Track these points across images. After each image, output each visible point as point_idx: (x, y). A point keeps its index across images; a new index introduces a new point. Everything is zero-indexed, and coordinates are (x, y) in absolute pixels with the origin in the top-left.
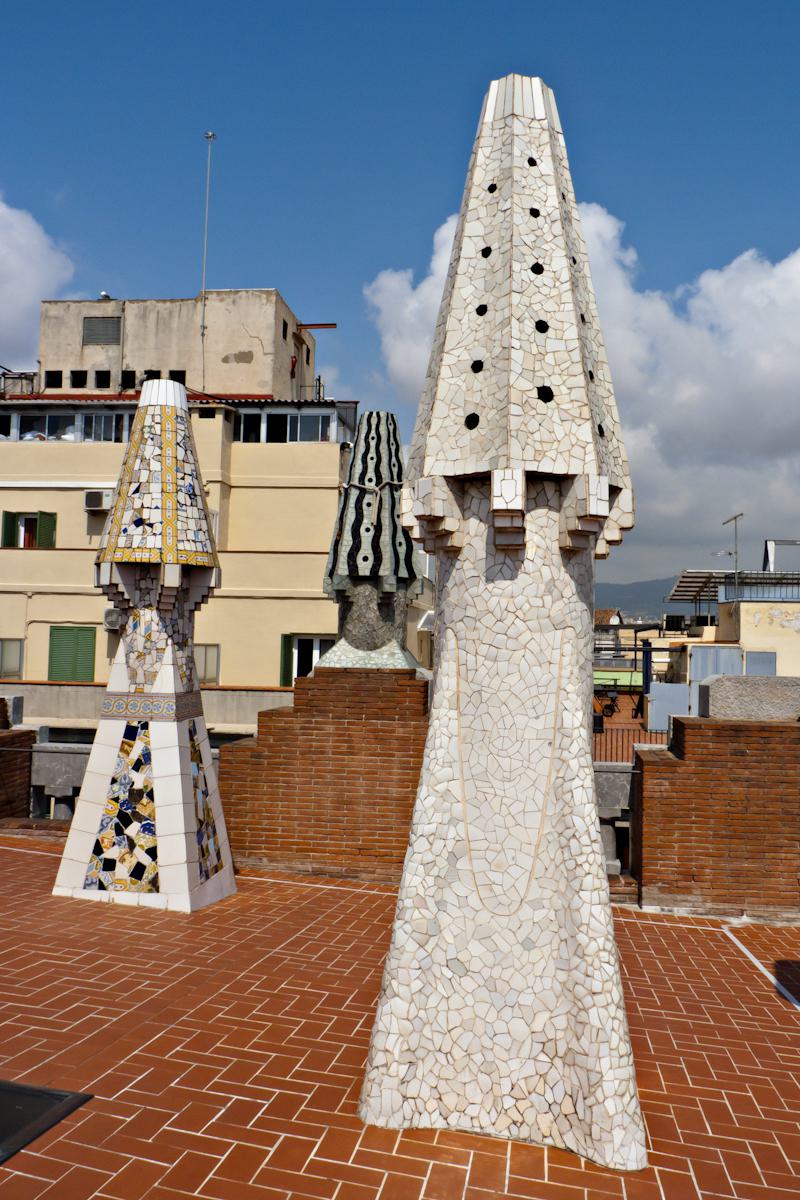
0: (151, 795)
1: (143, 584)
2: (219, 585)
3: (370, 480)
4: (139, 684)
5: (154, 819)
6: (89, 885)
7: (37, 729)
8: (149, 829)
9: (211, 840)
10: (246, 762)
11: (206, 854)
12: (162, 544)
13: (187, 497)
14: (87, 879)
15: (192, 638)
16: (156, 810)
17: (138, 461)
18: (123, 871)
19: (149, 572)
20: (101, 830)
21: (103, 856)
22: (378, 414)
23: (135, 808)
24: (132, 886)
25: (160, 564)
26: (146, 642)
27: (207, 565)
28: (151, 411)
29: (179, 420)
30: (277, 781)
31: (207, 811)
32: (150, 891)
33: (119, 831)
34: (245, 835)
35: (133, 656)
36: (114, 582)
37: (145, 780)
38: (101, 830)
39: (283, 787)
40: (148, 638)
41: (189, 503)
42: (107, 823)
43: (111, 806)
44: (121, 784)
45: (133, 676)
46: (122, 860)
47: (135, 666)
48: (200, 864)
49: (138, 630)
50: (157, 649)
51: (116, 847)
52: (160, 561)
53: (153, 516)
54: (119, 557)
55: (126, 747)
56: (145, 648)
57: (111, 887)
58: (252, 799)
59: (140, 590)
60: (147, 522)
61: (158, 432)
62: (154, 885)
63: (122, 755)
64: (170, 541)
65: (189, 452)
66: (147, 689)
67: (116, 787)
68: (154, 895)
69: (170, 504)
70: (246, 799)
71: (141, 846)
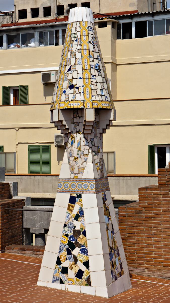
0: (84, 233)
1: (75, 120)
2: (115, 119)
4: (76, 174)
5: (87, 246)
6: (55, 281)
7: (25, 199)
8: (84, 251)
9: (117, 258)
10: (133, 216)
11: (115, 266)
12: (84, 98)
13: (96, 71)
14: (54, 278)
15: (102, 148)
16: (88, 241)
17: (69, 53)
18: (72, 274)
19: (78, 113)
20: (60, 251)
21: (61, 265)
23: (77, 240)
24: (77, 282)
25: (83, 109)
26: (78, 151)
27: (108, 108)
28: (74, 25)
29: (90, 29)
30: (151, 227)
31: (114, 242)
32: (86, 285)
33: (69, 253)
34: (134, 256)
35: (72, 159)
36: (60, 120)
37: (81, 225)
38: (60, 251)
39: (154, 230)
40: (79, 149)
41: (97, 75)
42: (63, 248)
43: (64, 239)
44: (69, 227)
45: (72, 169)
46: (71, 268)
47: (73, 165)
48: (112, 271)
49: (74, 145)
50: (84, 155)
51: (68, 261)
52: (83, 107)
53: (79, 83)
54: (62, 106)
55: (71, 207)
56: (78, 154)
57: (66, 282)
58: (138, 236)
59: (74, 123)
60: (76, 86)
61: (79, 37)
62: (88, 282)
63: (69, 212)
64: (88, 96)
65: (95, 46)
66: (80, 176)
67: (66, 229)
68: (88, 287)
69: (87, 76)
70: (134, 236)
71: (80, 260)
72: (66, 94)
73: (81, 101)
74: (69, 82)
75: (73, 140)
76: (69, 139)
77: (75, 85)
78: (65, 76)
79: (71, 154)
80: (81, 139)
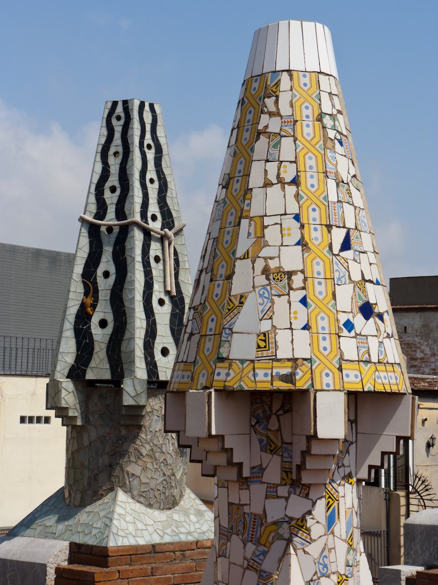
3: (154, 218)
17: (332, 184)
22: (152, 106)
26: (348, 552)
72: (357, 334)
73: (396, 365)
74: (357, 290)
75: (334, 508)
76: (314, 504)
77: (374, 306)
78: (337, 264)
79: (325, 566)
80: (353, 507)
